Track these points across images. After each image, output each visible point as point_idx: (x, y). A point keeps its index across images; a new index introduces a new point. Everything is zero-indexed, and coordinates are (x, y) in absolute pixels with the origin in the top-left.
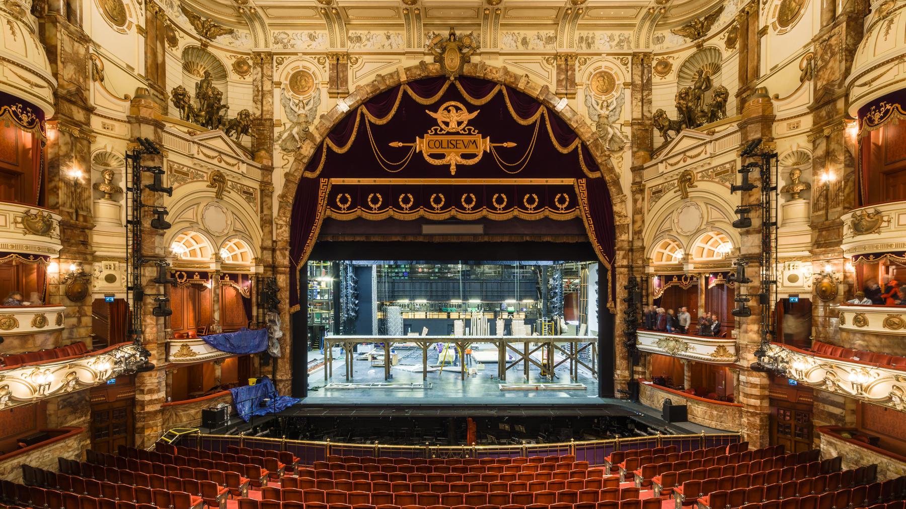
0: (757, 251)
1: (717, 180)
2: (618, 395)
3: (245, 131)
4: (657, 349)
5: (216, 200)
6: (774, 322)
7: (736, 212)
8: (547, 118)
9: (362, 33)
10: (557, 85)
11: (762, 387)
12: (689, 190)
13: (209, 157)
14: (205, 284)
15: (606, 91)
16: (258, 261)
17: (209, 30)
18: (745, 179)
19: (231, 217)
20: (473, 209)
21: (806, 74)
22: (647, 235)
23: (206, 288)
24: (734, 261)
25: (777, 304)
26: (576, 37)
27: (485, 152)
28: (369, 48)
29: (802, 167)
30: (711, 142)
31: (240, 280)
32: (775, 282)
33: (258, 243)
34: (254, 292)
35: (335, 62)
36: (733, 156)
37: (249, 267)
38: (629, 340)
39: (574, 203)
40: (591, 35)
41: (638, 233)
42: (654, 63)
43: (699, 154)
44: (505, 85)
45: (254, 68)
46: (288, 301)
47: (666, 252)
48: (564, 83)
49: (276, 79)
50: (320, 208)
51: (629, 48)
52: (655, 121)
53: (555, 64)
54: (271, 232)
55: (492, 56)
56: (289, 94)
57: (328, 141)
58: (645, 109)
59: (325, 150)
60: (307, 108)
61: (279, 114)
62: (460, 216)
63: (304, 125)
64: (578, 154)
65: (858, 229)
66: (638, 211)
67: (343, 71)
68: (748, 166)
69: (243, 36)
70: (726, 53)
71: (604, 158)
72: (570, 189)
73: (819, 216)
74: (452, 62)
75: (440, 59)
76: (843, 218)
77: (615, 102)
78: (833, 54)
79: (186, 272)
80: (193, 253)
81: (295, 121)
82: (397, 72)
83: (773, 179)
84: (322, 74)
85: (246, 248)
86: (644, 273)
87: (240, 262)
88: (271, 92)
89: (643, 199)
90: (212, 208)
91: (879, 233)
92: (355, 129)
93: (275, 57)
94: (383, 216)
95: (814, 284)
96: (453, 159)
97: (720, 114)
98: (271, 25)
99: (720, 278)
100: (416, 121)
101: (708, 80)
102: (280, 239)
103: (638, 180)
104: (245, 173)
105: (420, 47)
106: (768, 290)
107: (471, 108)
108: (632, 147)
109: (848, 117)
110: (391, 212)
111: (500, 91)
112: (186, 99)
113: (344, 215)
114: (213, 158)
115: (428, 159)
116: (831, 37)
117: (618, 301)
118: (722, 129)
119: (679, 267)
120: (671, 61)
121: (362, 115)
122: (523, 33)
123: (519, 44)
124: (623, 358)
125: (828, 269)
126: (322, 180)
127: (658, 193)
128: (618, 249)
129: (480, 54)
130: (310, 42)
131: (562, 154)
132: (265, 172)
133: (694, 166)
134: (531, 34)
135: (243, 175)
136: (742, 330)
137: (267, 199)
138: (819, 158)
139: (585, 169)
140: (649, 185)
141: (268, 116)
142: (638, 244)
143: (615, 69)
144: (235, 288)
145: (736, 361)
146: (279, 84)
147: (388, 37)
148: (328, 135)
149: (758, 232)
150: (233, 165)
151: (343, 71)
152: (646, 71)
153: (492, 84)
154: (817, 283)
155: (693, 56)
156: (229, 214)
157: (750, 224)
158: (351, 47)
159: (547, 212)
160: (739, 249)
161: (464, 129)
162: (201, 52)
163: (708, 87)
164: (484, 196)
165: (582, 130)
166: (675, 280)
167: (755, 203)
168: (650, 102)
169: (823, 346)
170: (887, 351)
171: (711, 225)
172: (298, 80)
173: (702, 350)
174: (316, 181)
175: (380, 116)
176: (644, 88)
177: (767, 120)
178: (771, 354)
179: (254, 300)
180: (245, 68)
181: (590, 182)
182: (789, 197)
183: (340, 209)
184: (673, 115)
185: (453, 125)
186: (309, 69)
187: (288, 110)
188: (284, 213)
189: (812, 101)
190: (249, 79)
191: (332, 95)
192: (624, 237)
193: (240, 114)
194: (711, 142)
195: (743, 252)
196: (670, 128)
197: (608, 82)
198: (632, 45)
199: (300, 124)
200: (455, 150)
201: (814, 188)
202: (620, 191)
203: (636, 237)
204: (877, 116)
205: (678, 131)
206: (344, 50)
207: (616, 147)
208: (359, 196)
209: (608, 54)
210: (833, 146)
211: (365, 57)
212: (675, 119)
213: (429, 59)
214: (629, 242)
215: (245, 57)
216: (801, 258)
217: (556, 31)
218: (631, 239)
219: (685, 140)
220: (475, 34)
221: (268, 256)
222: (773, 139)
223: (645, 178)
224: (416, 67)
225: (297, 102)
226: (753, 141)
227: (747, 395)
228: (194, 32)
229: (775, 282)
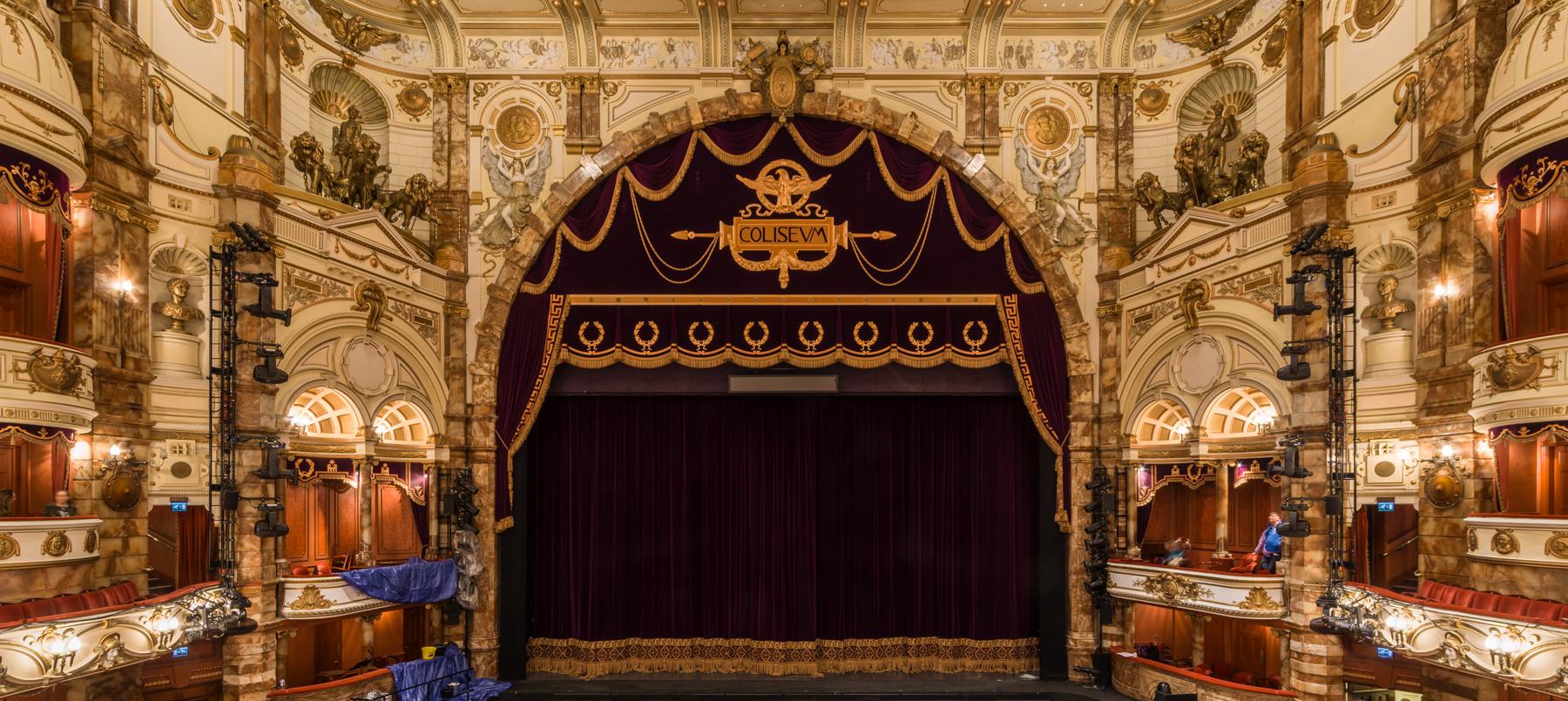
0: (1320, 420)
1: (1249, 297)
2: (1074, 677)
3: (418, 211)
4: (1144, 594)
5: (365, 332)
6: (1351, 547)
7: (1283, 353)
8: (949, 189)
9: (626, 40)
10: (967, 132)
11: (1331, 662)
12: (1199, 314)
13: (353, 256)
14: (346, 481)
15: (1054, 142)
16: (440, 440)
17: (358, 36)
18: (1299, 295)
19: (392, 363)
20: (819, 348)
21: (1406, 109)
22: (1126, 394)
23: (348, 487)
24: (1280, 438)
25: (1356, 514)
26: (1001, 48)
27: (840, 248)
28: (637, 66)
29: (1398, 273)
30: (1238, 229)
31: (408, 473)
32: (1353, 476)
33: (440, 408)
34: (433, 495)
35: (578, 92)
36: (1277, 254)
37: (425, 450)
38: (1094, 579)
39: (996, 338)
40: (1025, 45)
41: (1110, 390)
42: (1137, 93)
43: (1215, 253)
44: (876, 131)
45: (436, 101)
46: (492, 510)
47: (1160, 423)
48: (979, 127)
49: (473, 121)
50: (549, 346)
51: (1094, 66)
52: (1140, 193)
53: (962, 94)
54: (464, 389)
55: (853, 81)
56: (497, 147)
57: (565, 229)
58: (1122, 172)
59: (558, 245)
60: (528, 171)
61: (479, 181)
62: (796, 361)
63: (522, 202)
64: (1003, 252)
65: (1500, 381)
66: (1109, 352)
67: (591, 108)
68: (1303, 272)
69: (417, 45)
70: (1263, 75)
71: (1049, 259)
72: (989, 314)
73: (1429, 359)
74: (783, 91)
75: (761, 87)
76: (1473, 362)
77: (1068, 161)
78: (1453, 75)
79: (313, 459)
80: (326, 425)
81: (506, 194)
82: (686, 108)
83: (1349, 293)
84: (553, 112)
85: (420, 418)
86: (1120, 461)
87: (408, 442)
88: (465, 144)
89: (1118, 331)
90: (360, 347)
91: (1536, 388)
92: (612, 209)
93: (472, 83)
94: (660, 361)
95: (1422, 478)
96: (784, 260)
97: (1254, 181)
98: (465, 27)
99: (1255, 468)
100: (719, 194)
101: (1232, 121)
102: (478, 400)
103: (1109, 296)
104: (420, 285)
105: (725, 64)
106: (1340, 490)
107: (815, 172)
108: (1098, 239)
109: (1479, 183)
110: (675, 354)
111: (867, 142)
112: (316, 156)
113: (593, 359)
114: (363, 259)
115: (739, 260)
116: (1449, 44)
117: (1075, 509)
118: (1256, 208)
119: (1183, 450)
120: (1166, 88)
121: (625, 183)
122: (907, 40)
123: (900, 60)
124: (1084, 611)
125: (1447, 451)
126: (553, 297)
127: (1144, 320)
128: (1075, 419)
129: (832, 77)
130: (533, 57)
131: (975, 251)
132: (454, 284)
133: (1209, 272)
134: (920, 42)
135: (414, 288)
136: (1294, 561)
137: (458, 332)
138: (1428, 257)
139: (1016, 278)
140: (1128, 305)
141: (459, 186)
142: (1109, 409)
143: (1069, 102)
144: (399, 487)
145: (1285, 615)
146: (478, 130)
147: (671, 48)
148: (564, 219)
149: (1323, 387)
150: (398, 272)
151: (591, 108)
152: (1122, 107)
153: (852, 129)
154: (1427, 477)
155: (1206, 81)
156: (391, 358)
157: (1307, 374)
158: (607, 66)
159: (949, 353)
160: (1289, 417)
161: (803, 209)
162: (343, 75)
163: (1233, 134)
164: (838, 326)
165: (1011, 210)
166: (1175, 472)
167: (1316, 336)
168: (1130, 160)
169: (1438, 588)
170: (1552, 596)
171: (1238, 376)
172: (512, 124)
173: (1225, 597)
174: (542, 302)
175: (656, 185)
176: (1118, 137)
177: (1337, 191)
178: (1347, 603)
179: (433, 508)
180: (420, 101)
181: (1024, 300)
182: (1376, 325)
183: (584, 348)
184: (1171, 182)
185: (784, 202)
186: (532, 104)
187: (495, 176)
188: (487, 356)
189: (1416, 157)
190: (426, 120)
191: (572, 149)
192: (1085, 397)
193: (411, 182)
194: (1238, 229)
195: (1295, 424)
196: (1166, 206)
197: (1056, 125)
198: (1099, 62)
199: (513, 199)
200: (788, 244)
201: (1422, 309)
202: (1078, 316)
203: (1106, 397)
204: (1533, 181)
205: (1180, 211)
206: (594, 70)
207: (1070, 240)
208: (619, 326)
209: (1056, 77)
210: (1454, 236)
211: (629, 82)
212: (1175, 190)
213: (742, 86)
214: (1094, 405)
215: (419, 82)
216: (1398, 434)
217: (965, 36)
218: (1097, 401)
219: (1192, 226)
220: (823, 43)
221: (457, 432)
222: (1348, 224)
223: (1122, 294)
224: (719, 100)
225: (510, 160)
226: (1313, 227)
227: (1302, 676)
228: (331, 40)
229: (1353, 476)
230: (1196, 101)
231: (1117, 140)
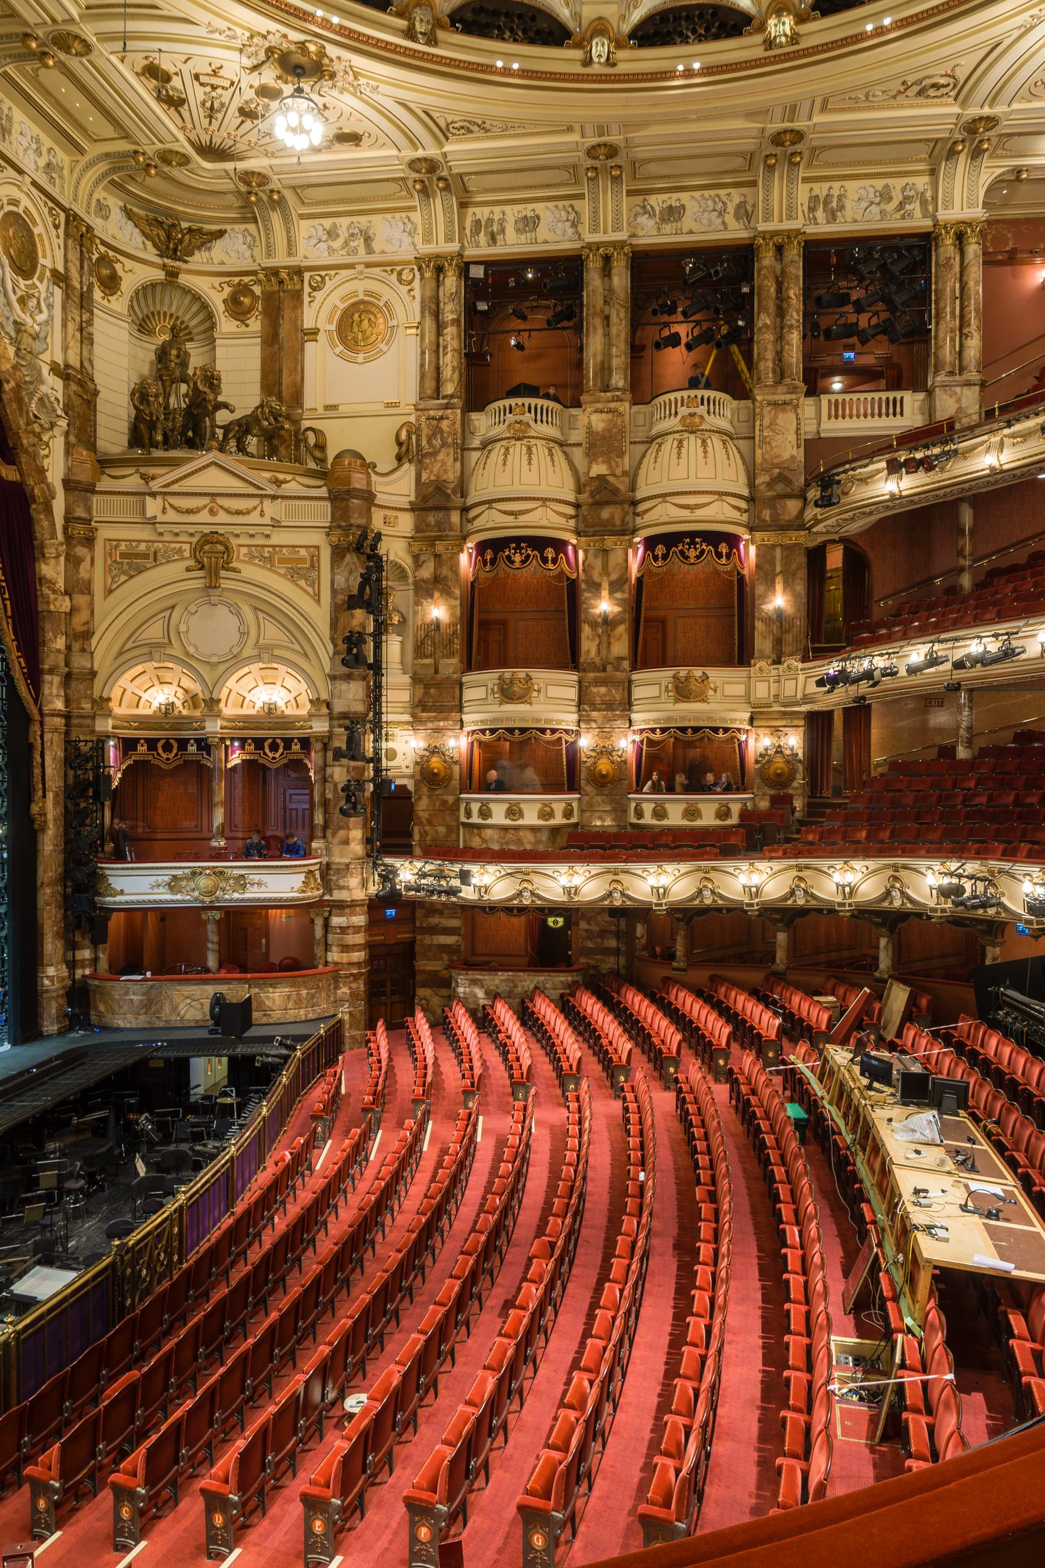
71: (33, 439)
103: (80, 512)
120: (118, 267)
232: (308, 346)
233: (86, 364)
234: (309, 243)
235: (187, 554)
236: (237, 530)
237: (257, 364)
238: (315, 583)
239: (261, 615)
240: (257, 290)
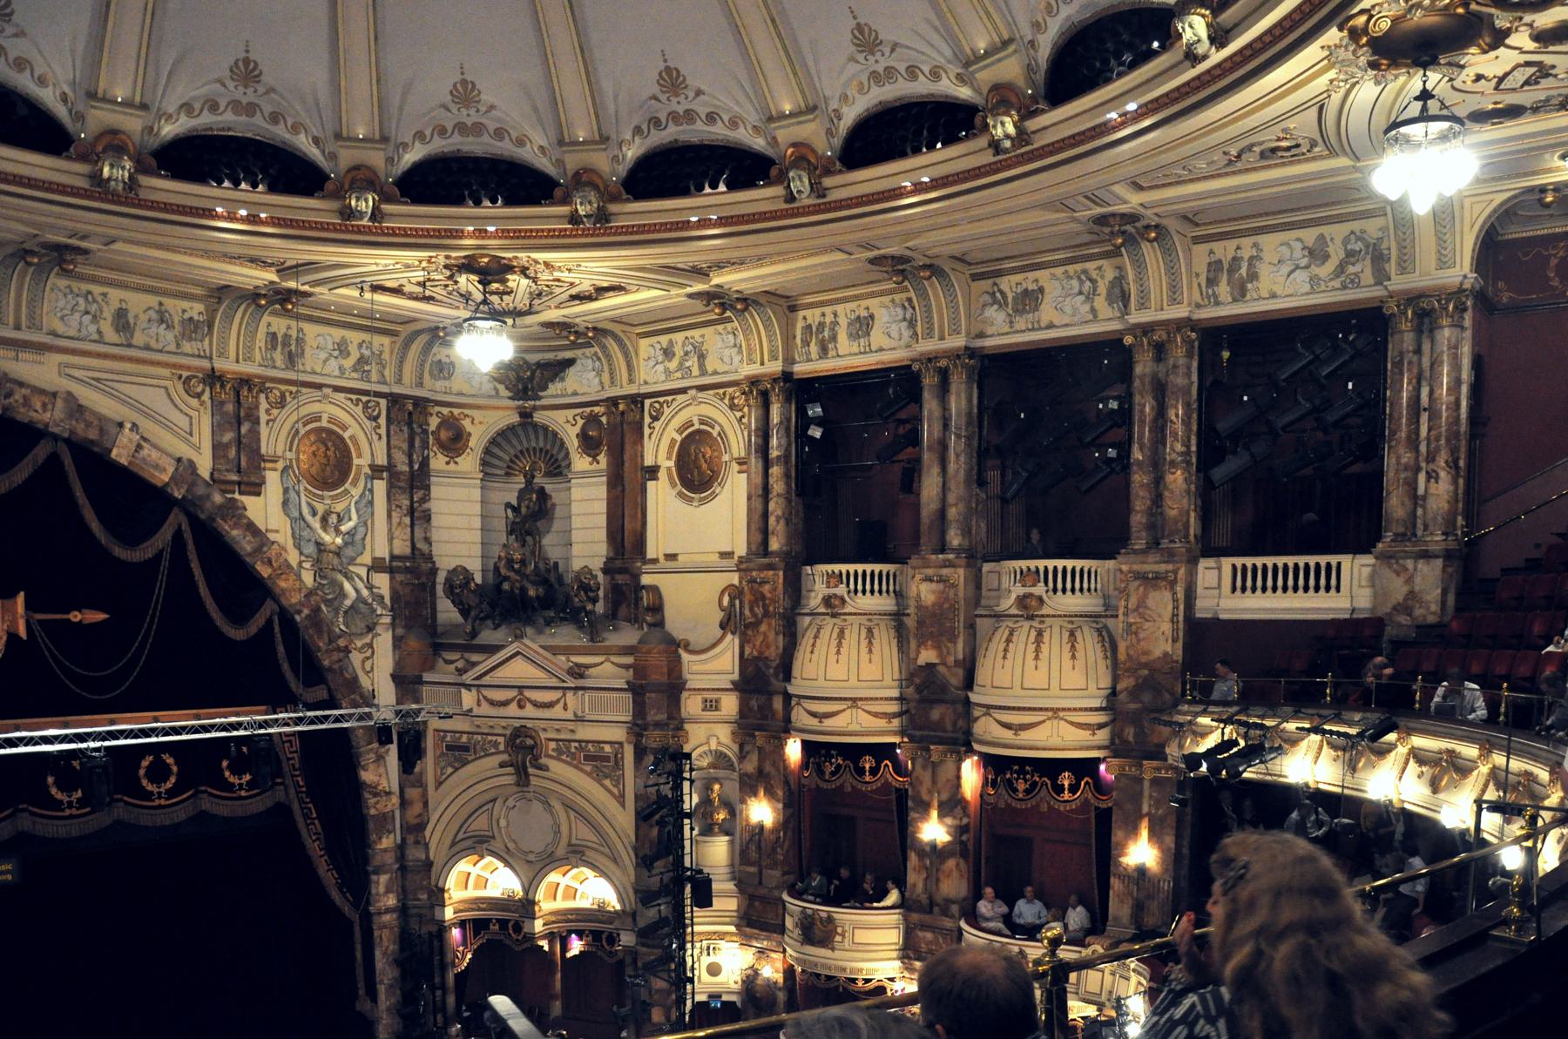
58: (419, 533)
71: (335, 656)
108: (393, 625)
139: (294, 685)
165: (283, 584)
168: (427, 517)
230: (498, 445)
231: (412, 487)
232: (650, 485)
233: (421, 545)
234: (651, 369)
235: (502, 747)
236: (542, 724)
237: (602, 507)
238: (619, 781)
239: (572, 814)
240: (604, 419)
